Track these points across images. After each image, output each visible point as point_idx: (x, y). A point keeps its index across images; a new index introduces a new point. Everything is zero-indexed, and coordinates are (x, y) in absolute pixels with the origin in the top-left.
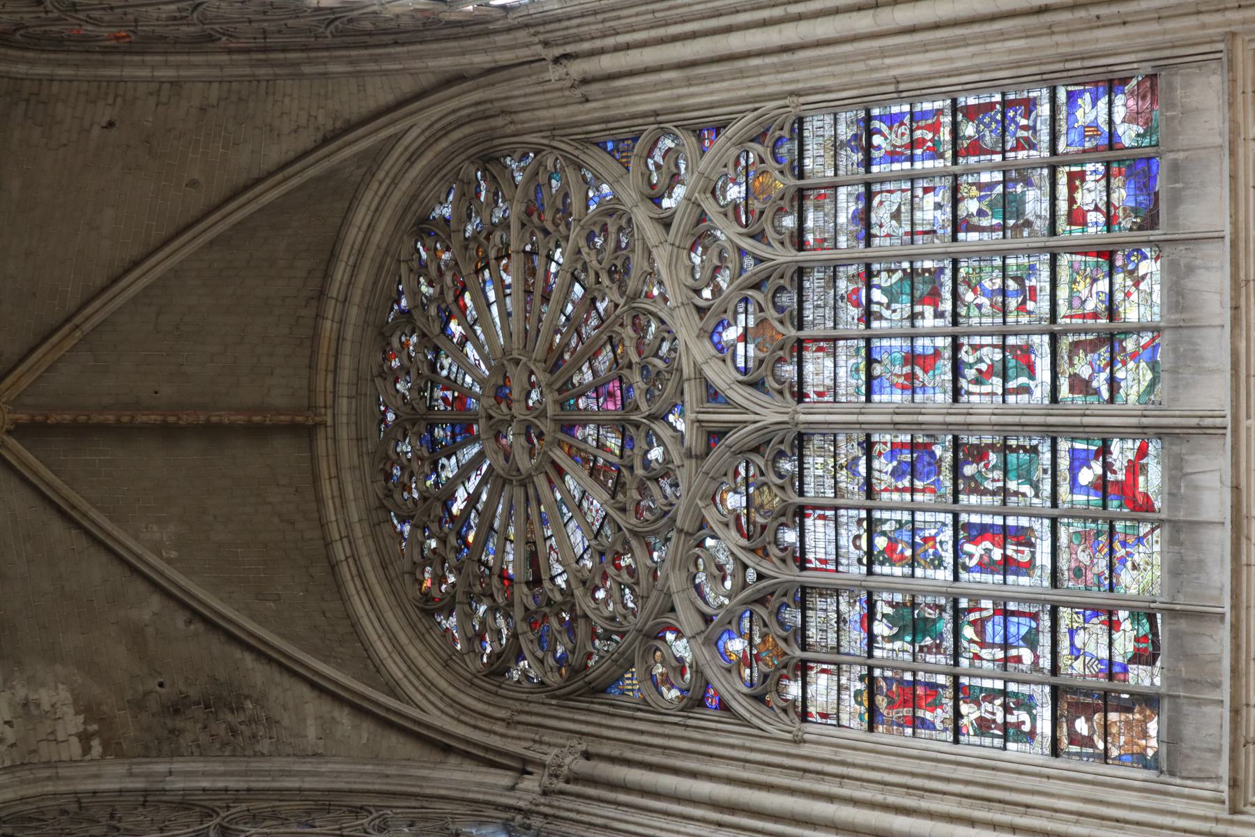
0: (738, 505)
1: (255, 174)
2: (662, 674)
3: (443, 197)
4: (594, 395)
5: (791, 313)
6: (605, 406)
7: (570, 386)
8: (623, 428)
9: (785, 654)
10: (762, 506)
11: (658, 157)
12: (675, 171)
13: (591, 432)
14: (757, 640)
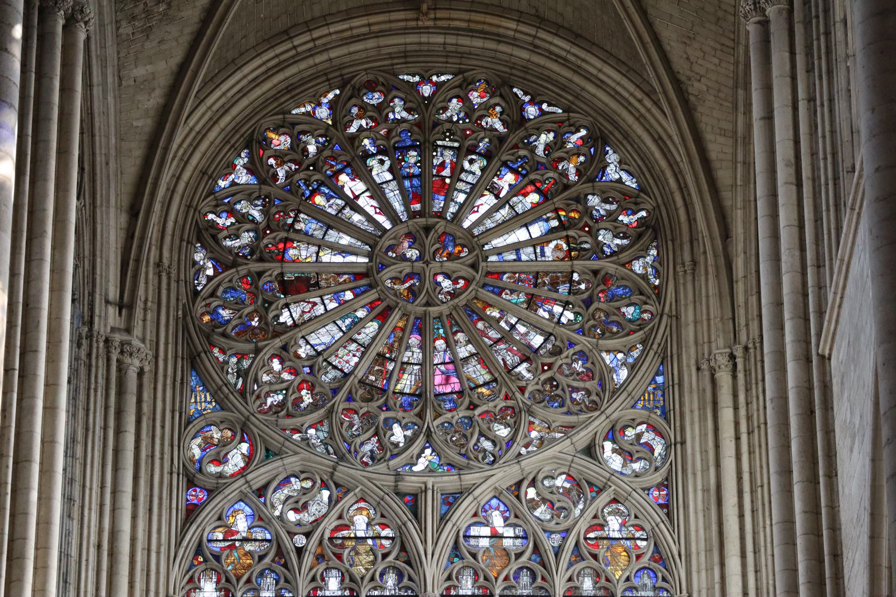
0: (358, 528)
1: (650, 11)
2: (212, 438)
3: (626, 167)
4: (447, 360)
5: (514, 587)
6: (438, 372)
7: (455, 329)
8: (419, 395)
9: (238, 580)
10: (357, 553)
11: (648, 437)
12: (636, 456)
13: (415, 356)
14: (248, 547)
